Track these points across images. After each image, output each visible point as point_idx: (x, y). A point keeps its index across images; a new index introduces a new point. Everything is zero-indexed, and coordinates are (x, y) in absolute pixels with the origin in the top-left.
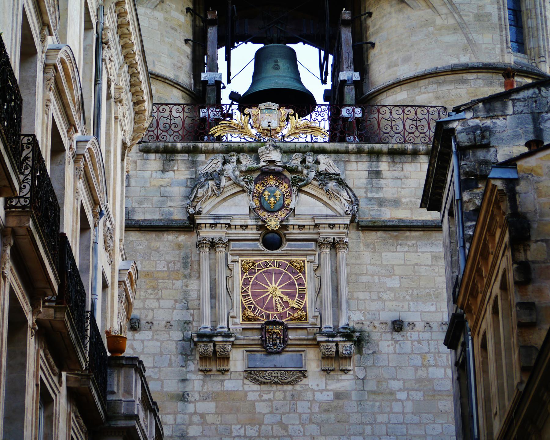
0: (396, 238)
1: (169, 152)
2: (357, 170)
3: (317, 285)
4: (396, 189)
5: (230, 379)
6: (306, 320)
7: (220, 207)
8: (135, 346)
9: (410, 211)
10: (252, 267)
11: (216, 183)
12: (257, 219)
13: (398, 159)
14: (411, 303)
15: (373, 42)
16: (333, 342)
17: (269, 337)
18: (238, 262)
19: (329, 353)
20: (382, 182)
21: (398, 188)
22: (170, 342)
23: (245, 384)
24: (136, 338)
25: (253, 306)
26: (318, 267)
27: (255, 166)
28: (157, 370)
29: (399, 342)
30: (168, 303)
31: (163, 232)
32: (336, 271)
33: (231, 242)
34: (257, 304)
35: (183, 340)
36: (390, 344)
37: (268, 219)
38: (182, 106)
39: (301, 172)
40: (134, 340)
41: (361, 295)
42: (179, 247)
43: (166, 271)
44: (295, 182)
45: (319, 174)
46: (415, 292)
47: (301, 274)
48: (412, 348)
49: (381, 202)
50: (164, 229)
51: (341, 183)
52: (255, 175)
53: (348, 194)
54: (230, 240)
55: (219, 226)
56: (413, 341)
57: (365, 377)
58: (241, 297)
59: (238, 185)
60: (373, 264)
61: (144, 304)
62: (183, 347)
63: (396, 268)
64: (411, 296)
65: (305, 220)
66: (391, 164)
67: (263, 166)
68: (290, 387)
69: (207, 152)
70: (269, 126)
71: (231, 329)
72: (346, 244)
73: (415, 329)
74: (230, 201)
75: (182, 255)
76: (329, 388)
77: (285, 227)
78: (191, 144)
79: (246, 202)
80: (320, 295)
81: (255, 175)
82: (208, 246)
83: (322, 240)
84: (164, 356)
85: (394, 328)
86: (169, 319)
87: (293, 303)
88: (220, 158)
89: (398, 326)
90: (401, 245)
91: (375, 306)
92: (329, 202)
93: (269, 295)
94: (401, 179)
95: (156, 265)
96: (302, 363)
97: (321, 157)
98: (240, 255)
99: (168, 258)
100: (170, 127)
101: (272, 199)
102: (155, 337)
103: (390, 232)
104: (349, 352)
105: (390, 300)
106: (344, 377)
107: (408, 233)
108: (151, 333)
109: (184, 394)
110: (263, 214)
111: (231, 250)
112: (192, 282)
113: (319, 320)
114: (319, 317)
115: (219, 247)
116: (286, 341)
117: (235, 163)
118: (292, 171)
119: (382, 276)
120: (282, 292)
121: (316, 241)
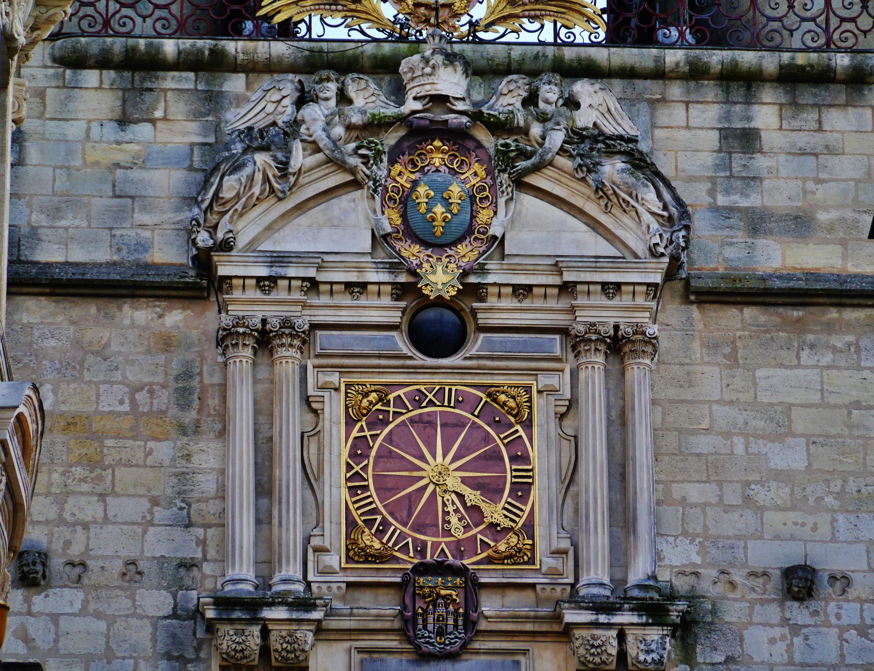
0: (799, 327)
1: (139, 67)
2: (688, 127)
3: (565, 461)
4: (800, 183)
6: (532, 561)
7: (287, 230)
8: (32, 632)
9: (839, 249)
10: (378, 406)
11: (275, 159)
12: (393, 268)
13: (806, 96)
14: (841, 518)
16: (609, 626)
18: (337, 390)
19: (597, 660)
20: (761, 162)
21: (805, 180)
22: (134, 622)
24: (35, 609)
25: (379, 518)
26: (569, 407)
27: (391, 111)
29: (804, 631)
30: (131, 508)
31: (121, 301)
32: (620, 422)
34: (391, 514)
35: (174, 615)
36: (778, 636)
39: (525, 131)
40: (30, 613)
41: (694, 492)
42: (167, 343)
43: (126, 413)
44: (505, 159)
45: (576, 136)
46: (852, 486)
47: (518, 427)
48: (841, 648)
49: (757, 223)
50: (124, 292)
51: (641, 164)
52: (391, 139)
53: (659, 196)
54: (314, 327)
56: (843, 629)
58: (345, 493)
59: (341, 165)
60: (731, 402)
61: (62, 509)
62: (174, 636)
63: (795, 413)
64: (839, 496)
65: (533, 272)
66: (788, 112)
67: (414, 112)
69: (253, 68)
71: (314, 586)
72: (652, 342)
73: (852, 593)
74: (316, 213)
75: (176, 367)
77: (476, 292)
78: (205, 44)
79: (362, 218)
80: (573, 489)
81: (391, 139)
82: (250, 342)
83: (582, 328)
84: (116, 663)
85: (789, 590)
86: (130, 551)
87: (494, 512)
88: (288, 85)
89: (800, 583)
90: (812, 346)
91: (733, 524)
92: (603, 219)
93: (425, 487)
94: (816, 155)
95: (98, 396)
97: (583, 89)
98: (343, 370)
99: (133, 375)
101: (439, 209)
102: (92, 607)
103: (781, 310)
104: (655, 656)
105: (778, 509)
107: (833, 314)
108: (81, 595)
110: (412, 252)
111: (318, 356)
113: (571, 563)
115: (283, 345)
116: (475, 624)
117: (333, 103)
118: (497, 127)
119: (756, 437)
120: (464, 481)
121: (563, 331)
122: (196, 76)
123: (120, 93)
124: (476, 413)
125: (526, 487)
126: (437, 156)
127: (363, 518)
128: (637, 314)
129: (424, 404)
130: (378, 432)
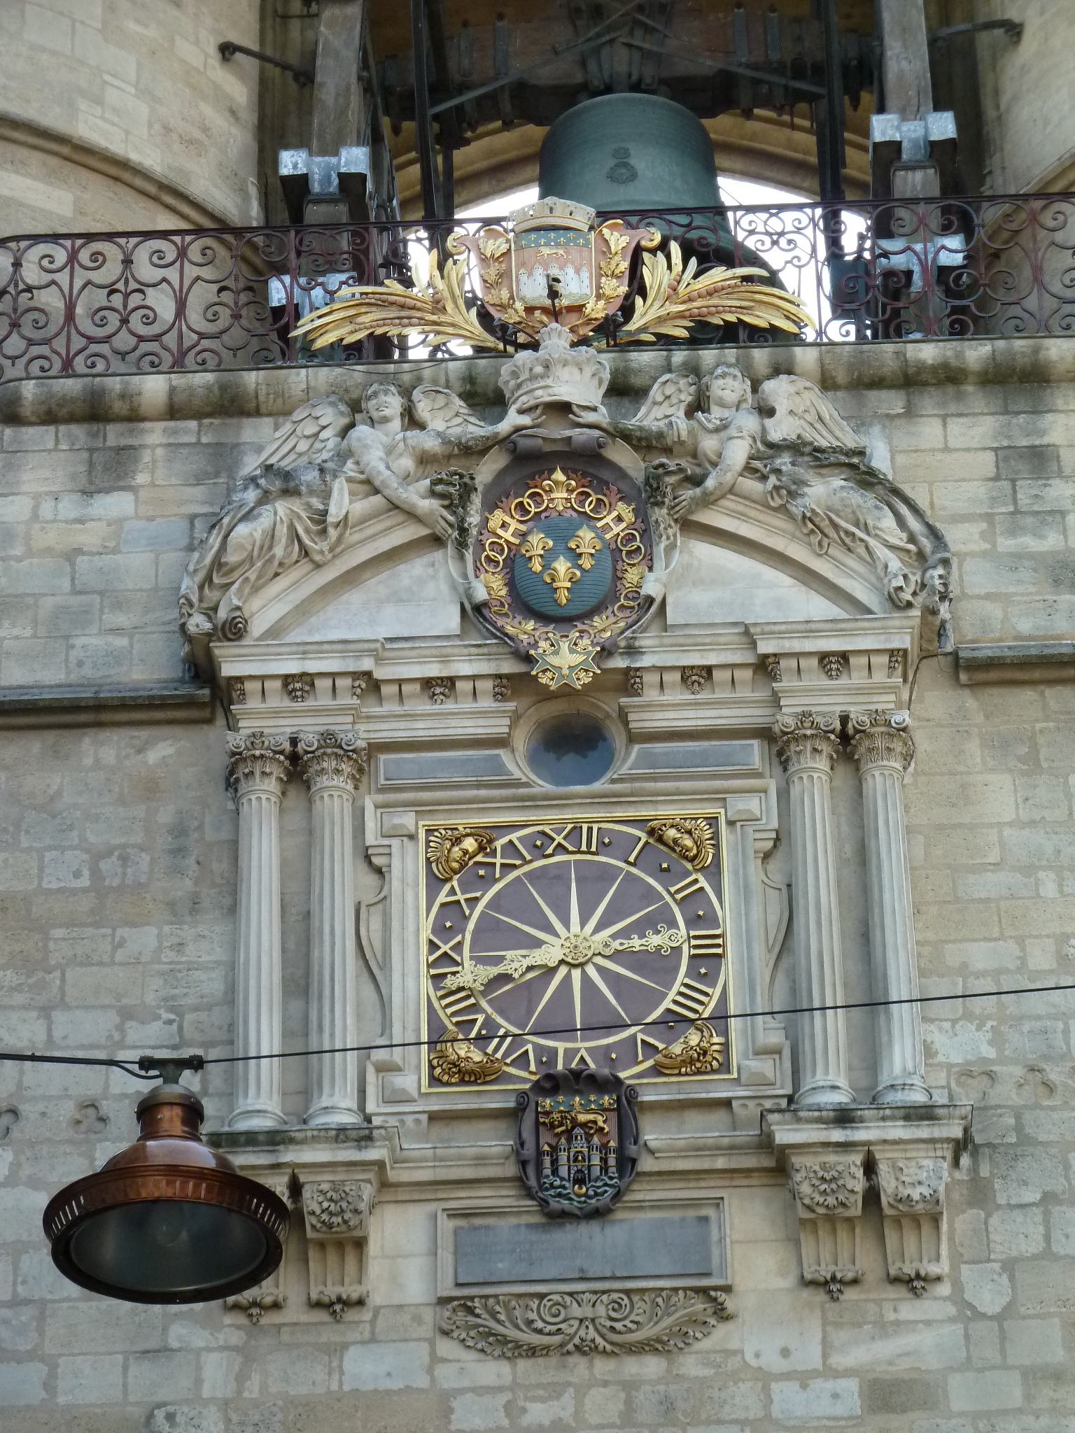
2: (946, 449)
3: (773, 919)
5: (373, 1340)
6: (725, 1067)
7: (330, 610)
10: (479, 858)
11: (309, 506)
15: (1017, 20)
16: (846, 1146)
17: (555, 1149)
18: (412, 837)
19: (831, 1201)
23: (444, 1360)
25: (481, 1018)
26: (777, 840)
28: (26, 1314)
33: (383, 757)
34: (501, 1012)
37: (543, 644)
38: (177, 239)
42: (150, 789)
43: (85, 891)
47: (700, 876)
54: (377, 748)
55: (323, 684)
57: (1008, 1312)
58: (426, 985)
60: (1032, 823)
65: (714, 646)
67: (518, 429)
68: (652, 1366)
70: (553, 294)
71: (376, 1121)
74: (377, 585)
76: (840, 1360)
79: (444, 588)
81: (486, 471)
82: (277, 771)
83: (791, 722)
95: (41, 869)
96: (707, 1258)
98: (421, 808)
100: (125, 321)
101: (562, 566)
102: (26, 1171)
106: (910, 1309)
109: (150, 1417)
110: (524, 629)
112: (202, 929)
113: (787, 1064)
114: (787, 1053)
116: (634, 1161)
117: (396, 424)
118: (644, 443)
121: (765, 734)
122: (200, 425)
123: (85, 455)
124: (631, 859)
125: (712, 962)
126: (559, 490)
127: (455, 1020)
128: (875, 698)
129: (550, 851)
130: (478, 894)
